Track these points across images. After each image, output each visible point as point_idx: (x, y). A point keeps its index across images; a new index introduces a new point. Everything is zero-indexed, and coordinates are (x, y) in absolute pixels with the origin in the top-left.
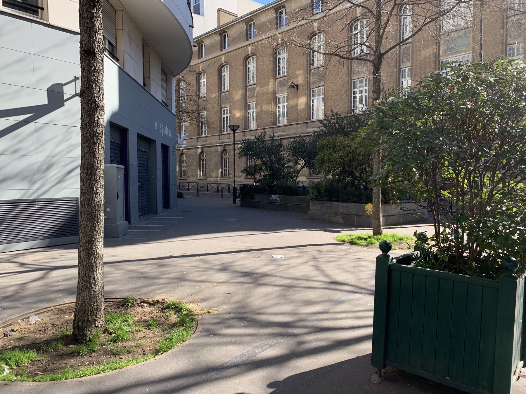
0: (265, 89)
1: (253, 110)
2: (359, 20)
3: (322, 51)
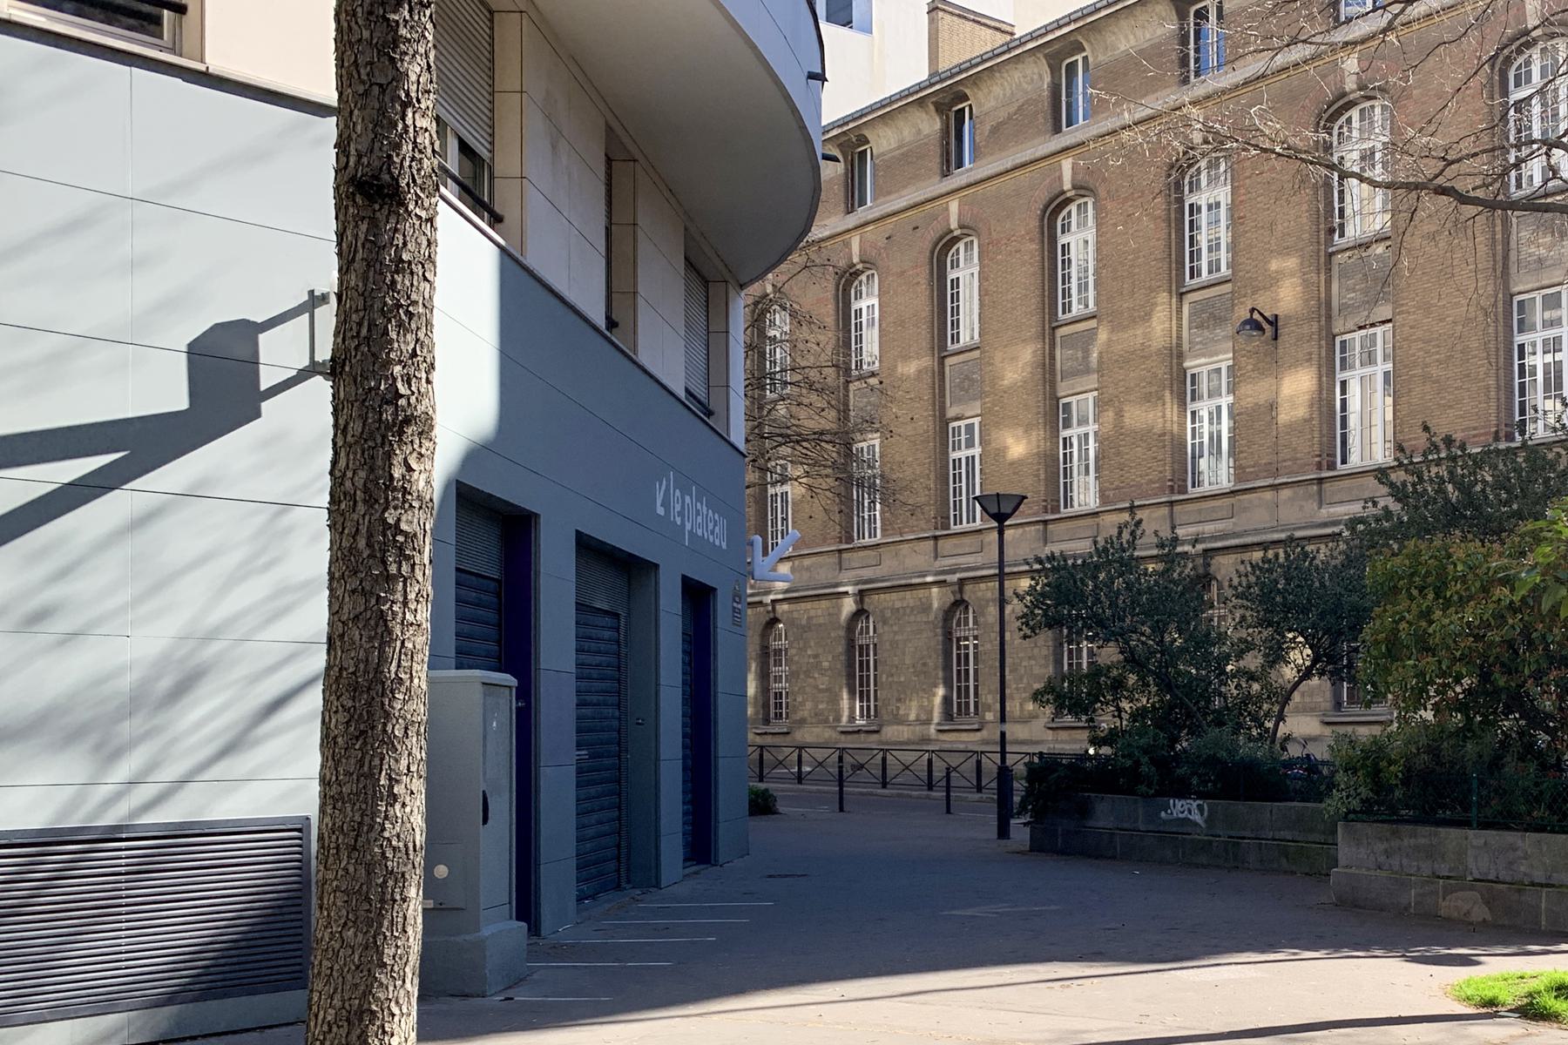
0: (1133, 337)
1: (1082, 430)
2: (1535, 41)
3: (1378, 173)
